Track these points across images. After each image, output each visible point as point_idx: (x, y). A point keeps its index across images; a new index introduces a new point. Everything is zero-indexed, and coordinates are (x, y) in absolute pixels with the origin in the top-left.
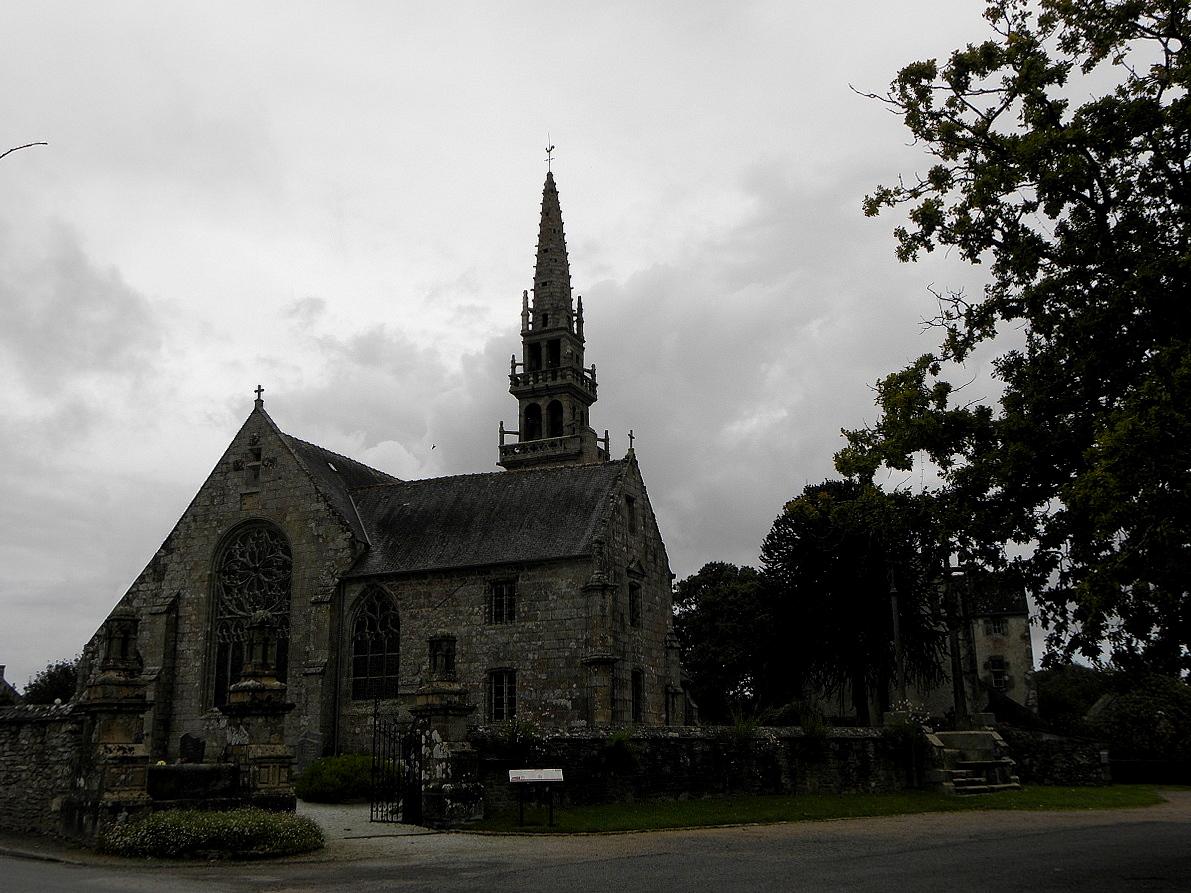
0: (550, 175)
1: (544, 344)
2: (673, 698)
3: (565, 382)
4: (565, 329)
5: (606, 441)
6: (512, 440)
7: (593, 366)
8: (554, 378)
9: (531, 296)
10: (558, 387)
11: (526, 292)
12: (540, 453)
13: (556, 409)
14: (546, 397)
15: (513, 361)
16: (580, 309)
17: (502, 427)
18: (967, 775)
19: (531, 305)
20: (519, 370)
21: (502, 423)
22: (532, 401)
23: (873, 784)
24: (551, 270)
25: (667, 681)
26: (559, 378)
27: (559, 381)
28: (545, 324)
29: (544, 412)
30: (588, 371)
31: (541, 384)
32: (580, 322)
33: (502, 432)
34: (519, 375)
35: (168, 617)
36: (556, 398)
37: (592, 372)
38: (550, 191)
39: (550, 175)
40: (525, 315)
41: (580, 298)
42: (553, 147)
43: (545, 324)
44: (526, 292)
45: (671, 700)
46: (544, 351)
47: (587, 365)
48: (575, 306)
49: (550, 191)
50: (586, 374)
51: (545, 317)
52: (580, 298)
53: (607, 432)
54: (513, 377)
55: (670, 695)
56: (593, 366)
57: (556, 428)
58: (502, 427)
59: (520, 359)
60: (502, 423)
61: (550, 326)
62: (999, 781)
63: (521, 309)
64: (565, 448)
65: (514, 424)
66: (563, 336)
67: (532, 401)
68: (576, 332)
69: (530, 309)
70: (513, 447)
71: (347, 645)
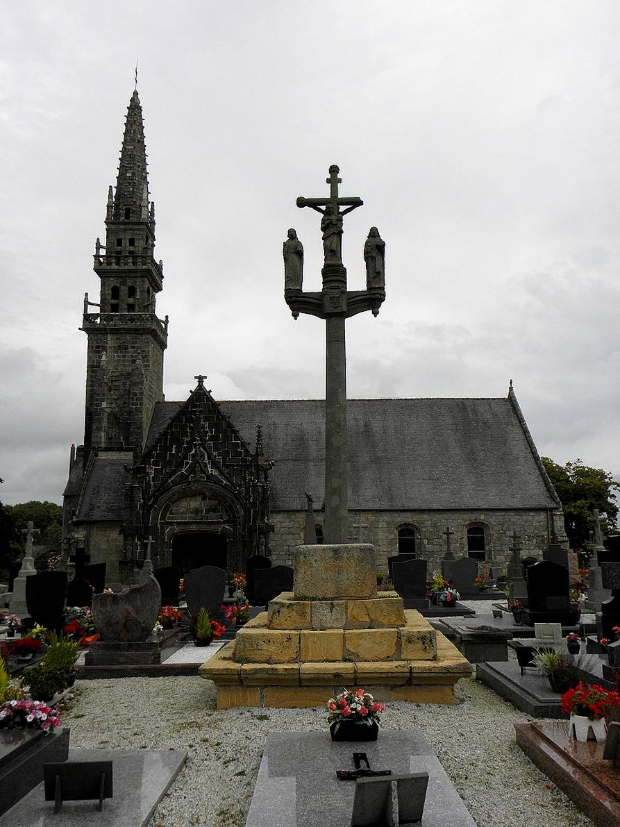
0: (136, 93)
4: (146, 224)
9: (114, 191)
20: (103, 252)
21: (86, 294)
28: (127, 217)
33: (87, 303)
34: (102, 256)
38: (135, 109)
39: (136, 93)
43: (127, 217)
44: (111, 187)
49: (135, 109)
53: (167, 317)
54: (97, 257)
59: (103, 242)
60: (86, 294)
65: (96, 298)
70: (96, 316)
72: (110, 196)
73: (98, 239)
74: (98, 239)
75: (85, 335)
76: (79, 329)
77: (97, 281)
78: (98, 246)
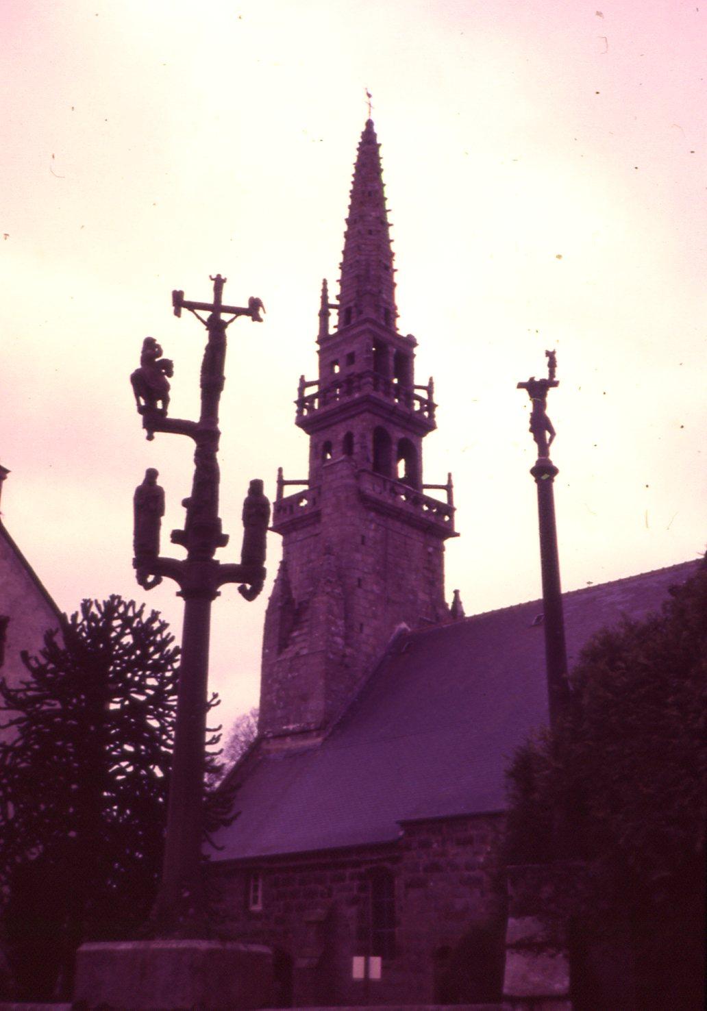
0: (369, 124)
5: (448, 488)
11: (325, 283)
19: (333, 300)
21: (280, 470)
37: (429, 389)
39: (369, 124)
40: (324, 315)
47: (420, 378)
50: (417, 392)
53: (450, 475)
54: (302, 402)
59: (313, 374)
60: (280, 470)
61: (353, 321)
63: (318, 306)
72: (325, 297)
77: (302, 441)
78: (304, 385)
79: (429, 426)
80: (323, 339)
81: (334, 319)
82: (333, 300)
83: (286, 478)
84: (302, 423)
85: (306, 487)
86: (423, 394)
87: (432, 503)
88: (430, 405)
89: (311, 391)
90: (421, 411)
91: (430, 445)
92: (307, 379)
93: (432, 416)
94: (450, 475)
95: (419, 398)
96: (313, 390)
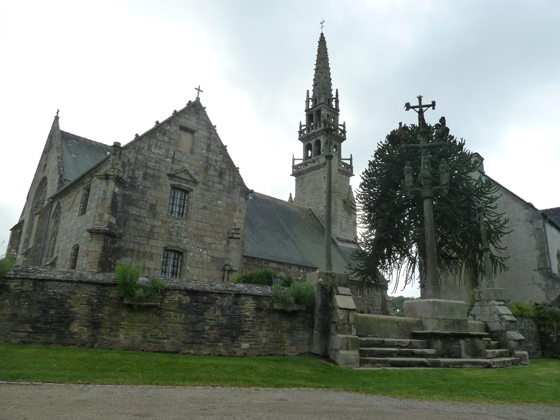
0: (322, 34)
1: (314, 113)
2: (228, 274)
3: (321, 128)
5: (351, 160)
6: (297, 163)
7: (344, 122)
8: (316, 128)
10: (318, 132)
11: (308, 91)
12: (308, 167)
13: (318, 143)
14: (314, 139)
15: (300, 124)
16: (337, 95)
17: (293, 157)
18: (410, 345)
19: (310, 97)
21: (293, 155)
22: (308, 142)
23: (245, 345)
24: (319, 77)
25: (226, 262)
26: (318, 127)
27: (319, 129)
29: (313, 146)
30: (341, 125)
31: (310, 133)
32: (337, 102)
35: (13, 232)
36: (318, 138)
37: (344, 126)
38: (322, 41)
39: (322, 34)
40: (307, 102)
41: (337, 90)
42: (324, 21)
44: (308, 91)
45: (226, 275)
46: (314, 117)
47: (341, 122)
48: (334, 93)
49: (322, 41)
50: (340, 127)
51: (316, 100)
52: (337, 90)
53: (351, 155)
54: (301, 132)
55: (226, 272)
56: (344, 122)
57: (318, 152)
58: (293, 157)
59: (304, 123)
60: (293, 155)
62: (463, 354)
64: (319, 162)
66: (322, 107)
67: (308, 142)
68: (334, 107)
69: (310, 99)
71: (49, 239)
72: (308, 96)
73: (301, 122)
74: (301, 122)
75: (294, 178)
76: (291, 175)
78: (301, 126)
79: (344, 139)
80: (307, 110)
81: (311, 103)
82: (310, 97)
83: (295, 158)
84: (300, 139)
85: (301, 161)
86: (342, 128)
87: (344, 164)
88: (344, 132)
89: (303, 128)
90: (341, 134)
91: (343, 144)
92: (302, 124)
93: (345, 135)
94: (351, 155)
95: (340, 130)
96: (305, 127)
